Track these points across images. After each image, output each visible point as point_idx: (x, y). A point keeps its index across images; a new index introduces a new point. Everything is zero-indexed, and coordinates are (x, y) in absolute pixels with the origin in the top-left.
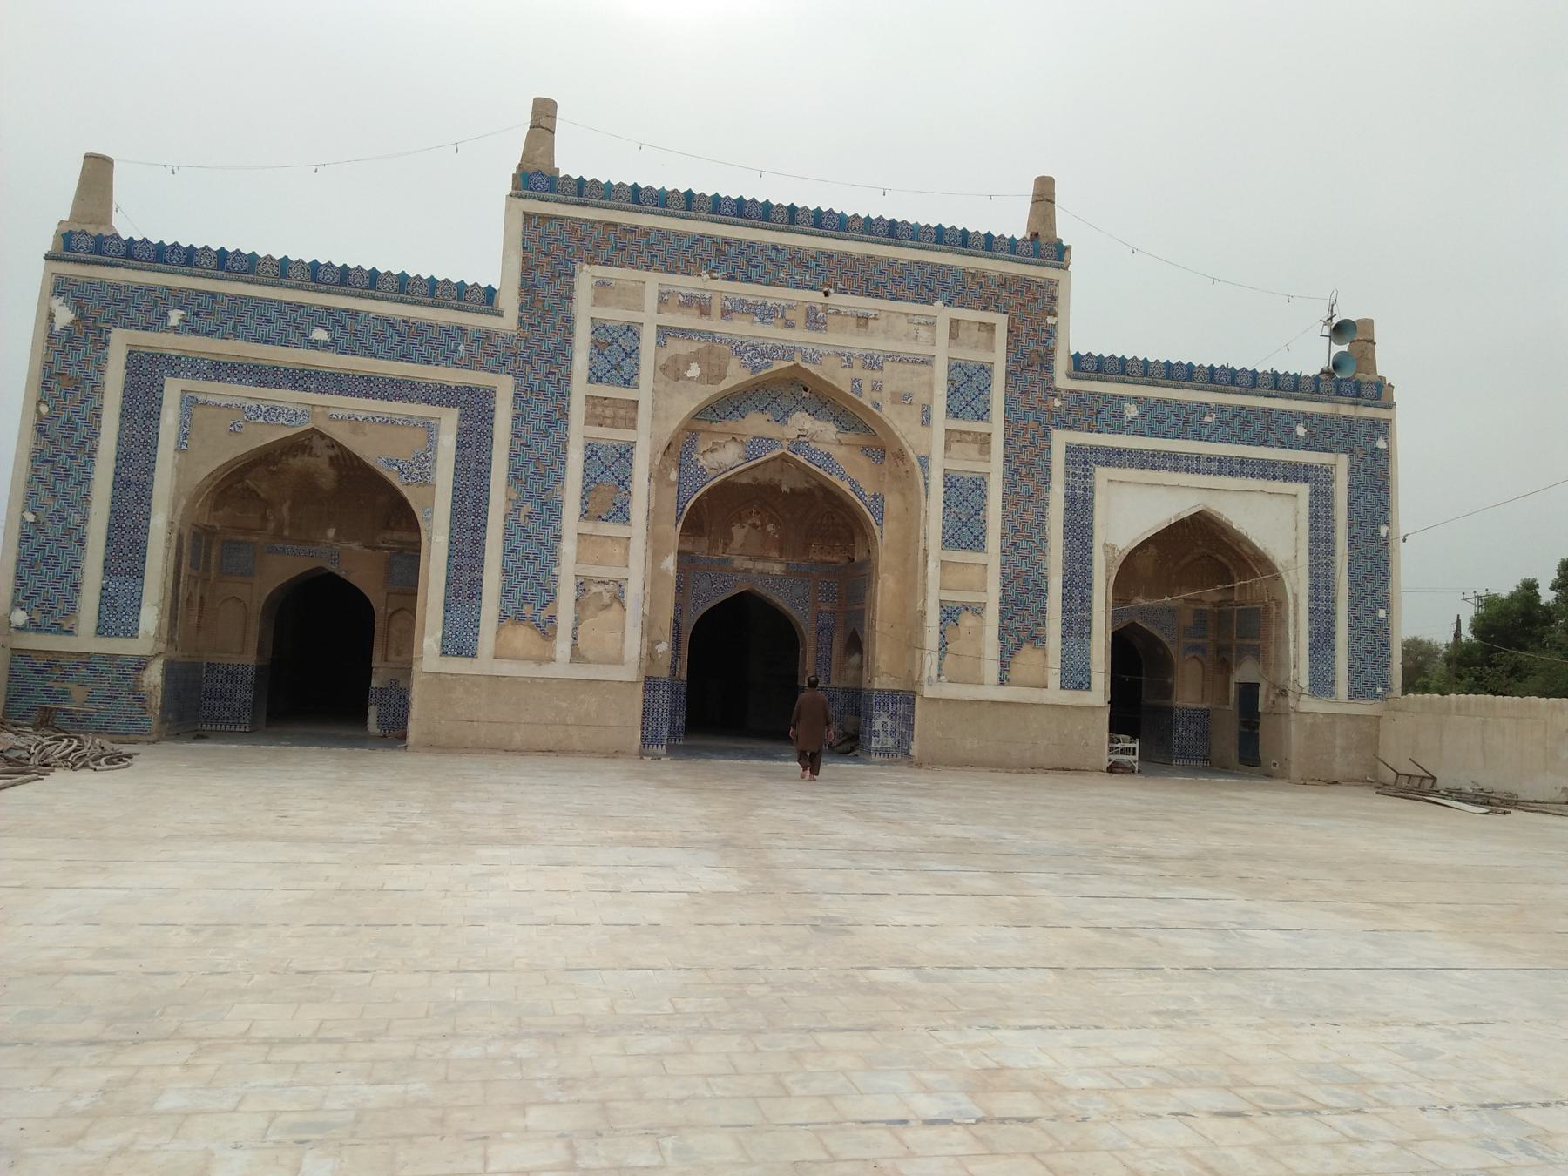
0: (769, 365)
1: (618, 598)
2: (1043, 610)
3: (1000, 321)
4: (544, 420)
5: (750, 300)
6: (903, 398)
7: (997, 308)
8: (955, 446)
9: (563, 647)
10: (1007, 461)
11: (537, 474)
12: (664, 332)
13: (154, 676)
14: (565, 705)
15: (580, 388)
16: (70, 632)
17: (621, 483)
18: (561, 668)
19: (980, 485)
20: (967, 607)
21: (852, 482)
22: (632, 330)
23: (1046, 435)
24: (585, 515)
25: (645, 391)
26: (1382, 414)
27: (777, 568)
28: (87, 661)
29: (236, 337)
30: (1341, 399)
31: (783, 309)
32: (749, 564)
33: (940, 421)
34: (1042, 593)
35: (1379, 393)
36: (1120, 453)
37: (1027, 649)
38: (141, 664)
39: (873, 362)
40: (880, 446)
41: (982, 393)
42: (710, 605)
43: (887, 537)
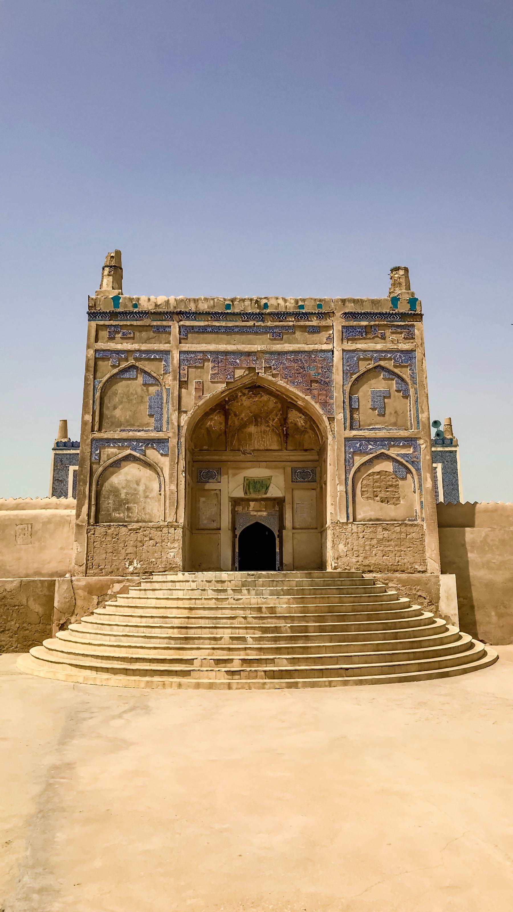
26: (453, 449)
27: (265, 514)
30: (437, 446)
32: (255, 513)
35: (452, 442)
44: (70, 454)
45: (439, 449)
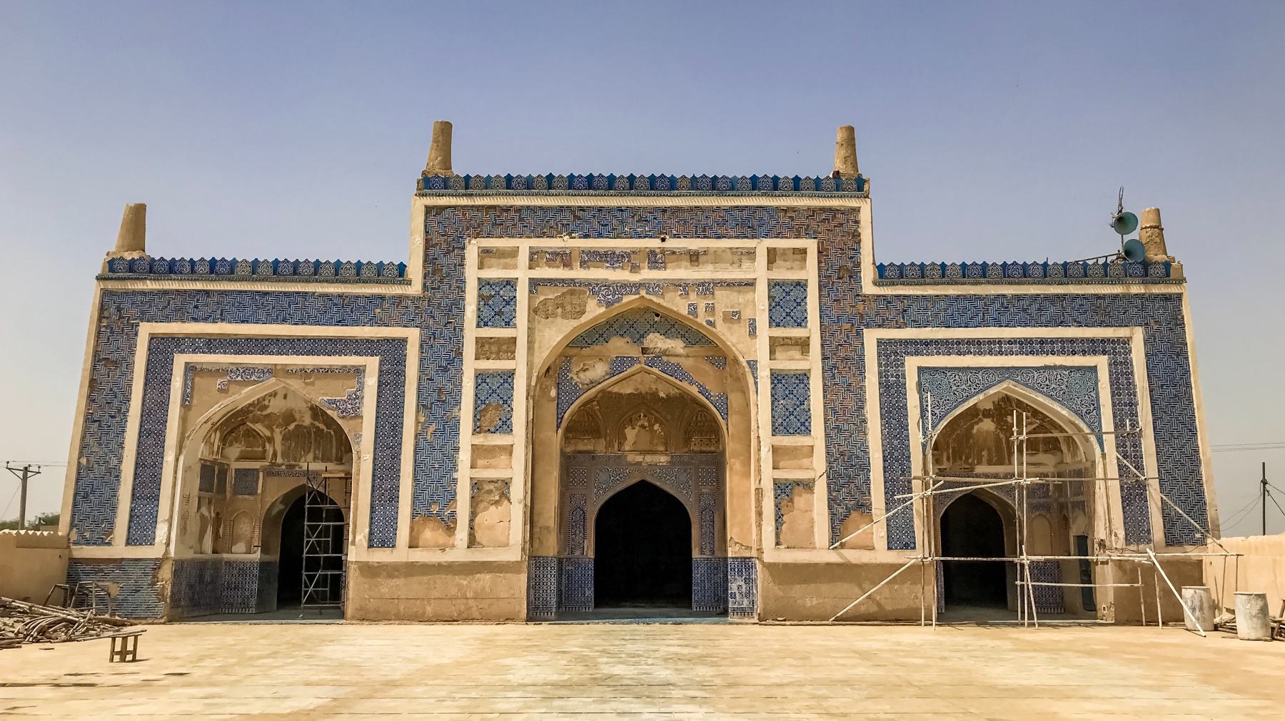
0: (619, 300)
1: (505, 496)
2: (867, 481)
3: (811, 245)
4: (442, 360)
5: (602, 251)
6: (733, 317)
7: (808, 235)
8: (778, 349)
9: (462, 534)
10: (824, 358)
11: (438, 402)
12: (535, 284)
13: (166, 573)
14: (465, 583)
15: (471, 332)
16: (109, 544)
17: (505, 402)
18: (459, 553)
19: (803, 378)
20: (798, 483)
21: (700, 386)
22: (511, 283)
23: (859, 334)
24: (477, 430)
25: (520, 331)
26: (1173, 290)
27: (663, 459)
28: (119, 562)
29: (223, 320)
30: (1130, 280)
31: (629, 255)
32: (639, 458)
33: (765, 332)
34: (865, 468)
35: (1168, 272)
36: (927, 343)
37: (854, 515)
38: (157, 564)
39: (706, 287)
40: (721, 358)
41: (799, 304)
42: (610, 494)
43: (730, 428)
44: (143, 293)
45: (1135, 289)
